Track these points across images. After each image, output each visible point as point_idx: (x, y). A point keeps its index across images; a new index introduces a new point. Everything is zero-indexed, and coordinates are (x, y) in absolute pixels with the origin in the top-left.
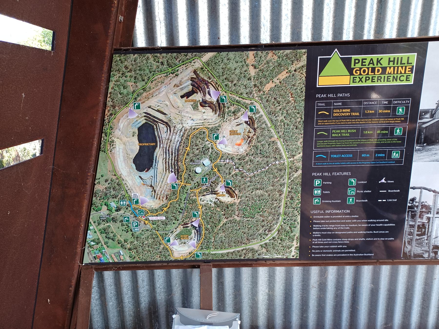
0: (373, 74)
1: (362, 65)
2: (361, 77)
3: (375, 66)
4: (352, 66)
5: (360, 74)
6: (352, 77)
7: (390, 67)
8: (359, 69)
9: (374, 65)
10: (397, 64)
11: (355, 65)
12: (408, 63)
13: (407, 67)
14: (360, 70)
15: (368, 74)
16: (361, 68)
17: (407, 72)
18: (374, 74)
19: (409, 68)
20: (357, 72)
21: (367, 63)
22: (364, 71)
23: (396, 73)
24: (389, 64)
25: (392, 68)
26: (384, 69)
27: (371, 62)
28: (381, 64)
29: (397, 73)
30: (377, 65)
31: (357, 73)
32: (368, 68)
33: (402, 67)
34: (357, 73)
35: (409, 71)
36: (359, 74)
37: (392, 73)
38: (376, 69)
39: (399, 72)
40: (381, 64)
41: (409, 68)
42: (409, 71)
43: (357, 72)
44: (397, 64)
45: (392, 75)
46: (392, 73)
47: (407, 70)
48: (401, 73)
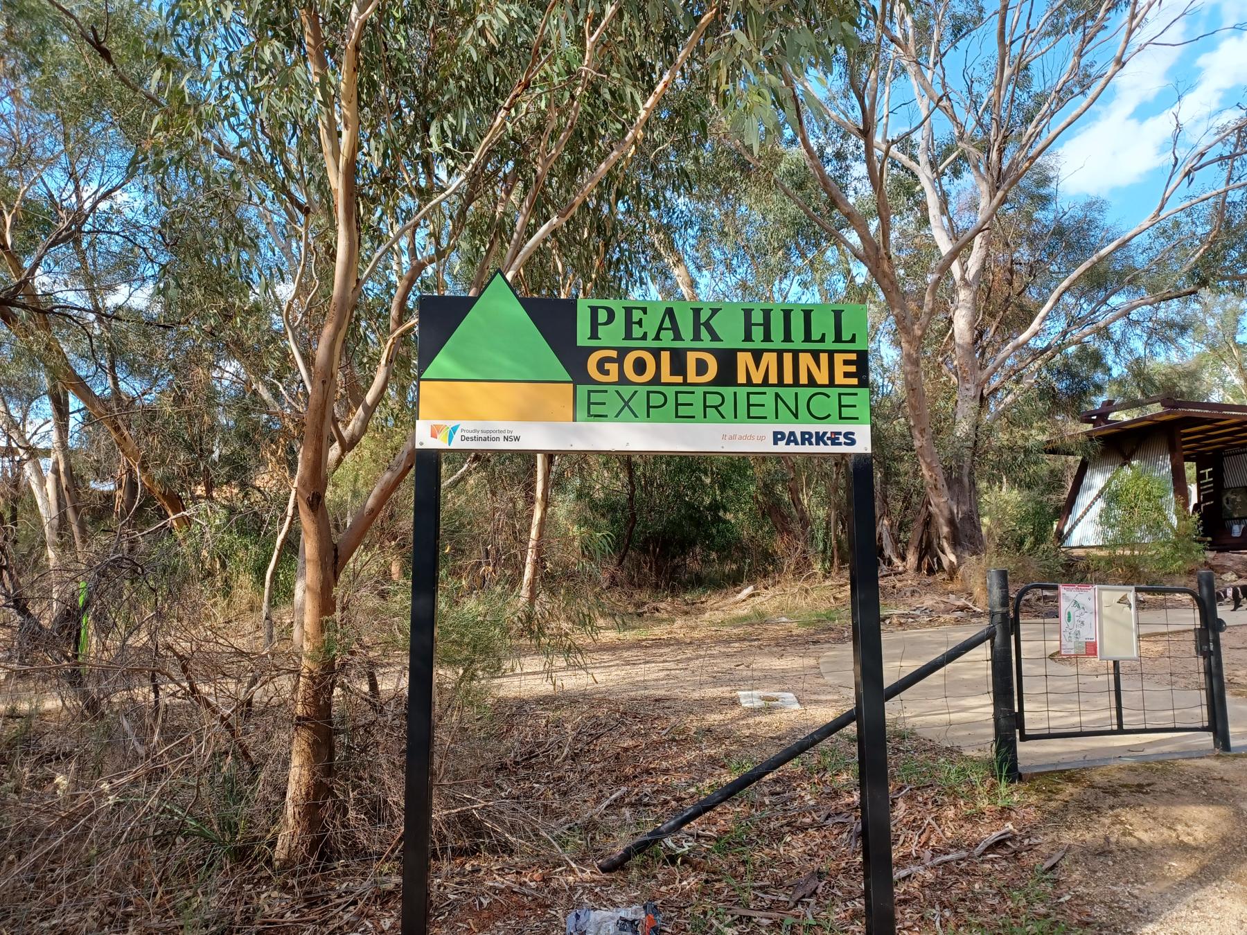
0: (679, 379)
1: (628, 336)
2: (626, 391)
3: (687, 342)
4: (583, 339)
5: (623, 380)
6: (583, 389)
7: (757, 355)
8: (614, 354)
9: (677, 337)
10: (787, 338)
11: (594, 335)
12: (838, 339)
13: (839, 358)
14: (620, 360)
15: (656, 380)
16: (623, 352)
17: (839, 379)
18: (685, 383)
19: (846, 362)
20: (607, 366)
21: (651, 325)
22: (640, 366)
23: (788, 379)
24: (748, 338)
25: (770, 359)
26: (727, 359)
27: (667, 324)
28: (715, 338)
29: (796, 383)
30: (697, 337)
31: (607, 373)
32: (656, 353)
33: (816, 355)
34: (607, 373)
35: (847, 375)
36: (614, 376)
37: (773, 379)
38: (691, 358)
39: (804, 379)
40: (715, 338)
41: (846, 362)
42: (847, 375)
43: (607, 366)
44: (787, 338)
45: (771, 391)
46: (773, 379)
47: (840, 369)
48: (812, 382)
